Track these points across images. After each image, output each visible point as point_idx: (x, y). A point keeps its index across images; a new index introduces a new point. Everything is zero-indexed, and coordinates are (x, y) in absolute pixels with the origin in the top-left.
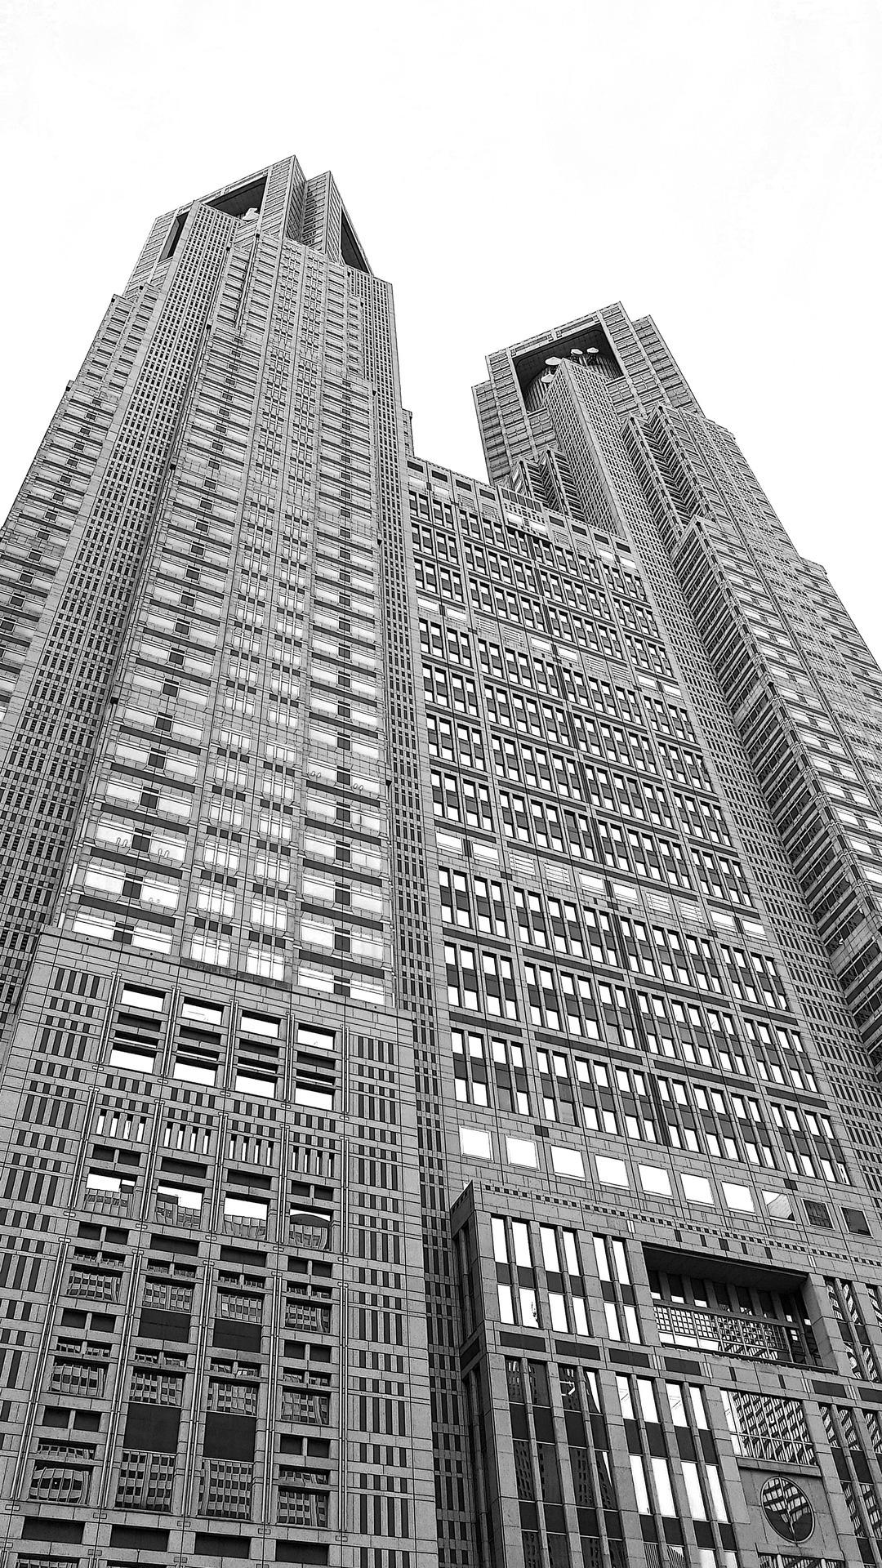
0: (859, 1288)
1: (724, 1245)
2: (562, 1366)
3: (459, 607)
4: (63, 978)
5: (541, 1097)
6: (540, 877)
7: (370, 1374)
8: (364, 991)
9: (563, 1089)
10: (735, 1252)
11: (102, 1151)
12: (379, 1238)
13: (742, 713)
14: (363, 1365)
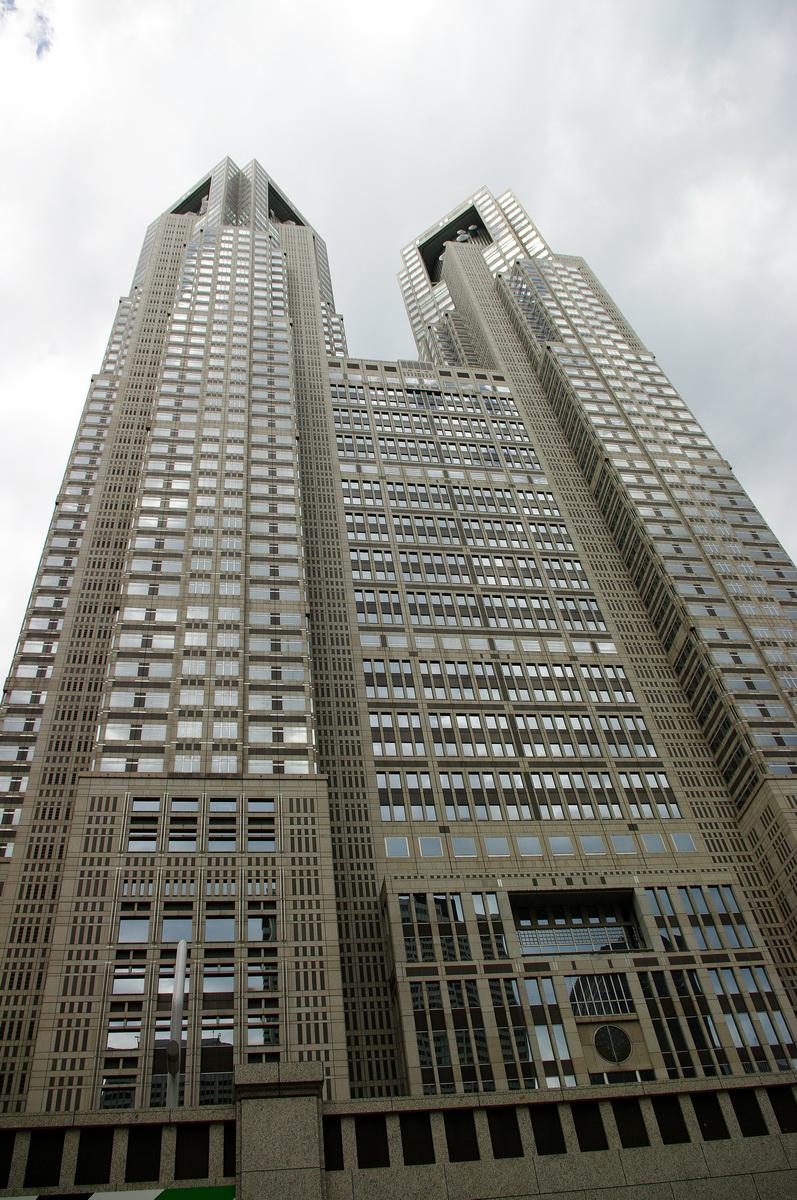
0: (673, 890)
1: (569, 881)
2: (450, 983)
3: (372, 462)
4: (96, 803)
5: (443, 805)
6: (439, 648)
7: (303, 1010)
8: (298, 767)
10: (578, 885)
11: (127, 906)
12: (307, 927)
13: (594, 484)
14: (299, 1005)
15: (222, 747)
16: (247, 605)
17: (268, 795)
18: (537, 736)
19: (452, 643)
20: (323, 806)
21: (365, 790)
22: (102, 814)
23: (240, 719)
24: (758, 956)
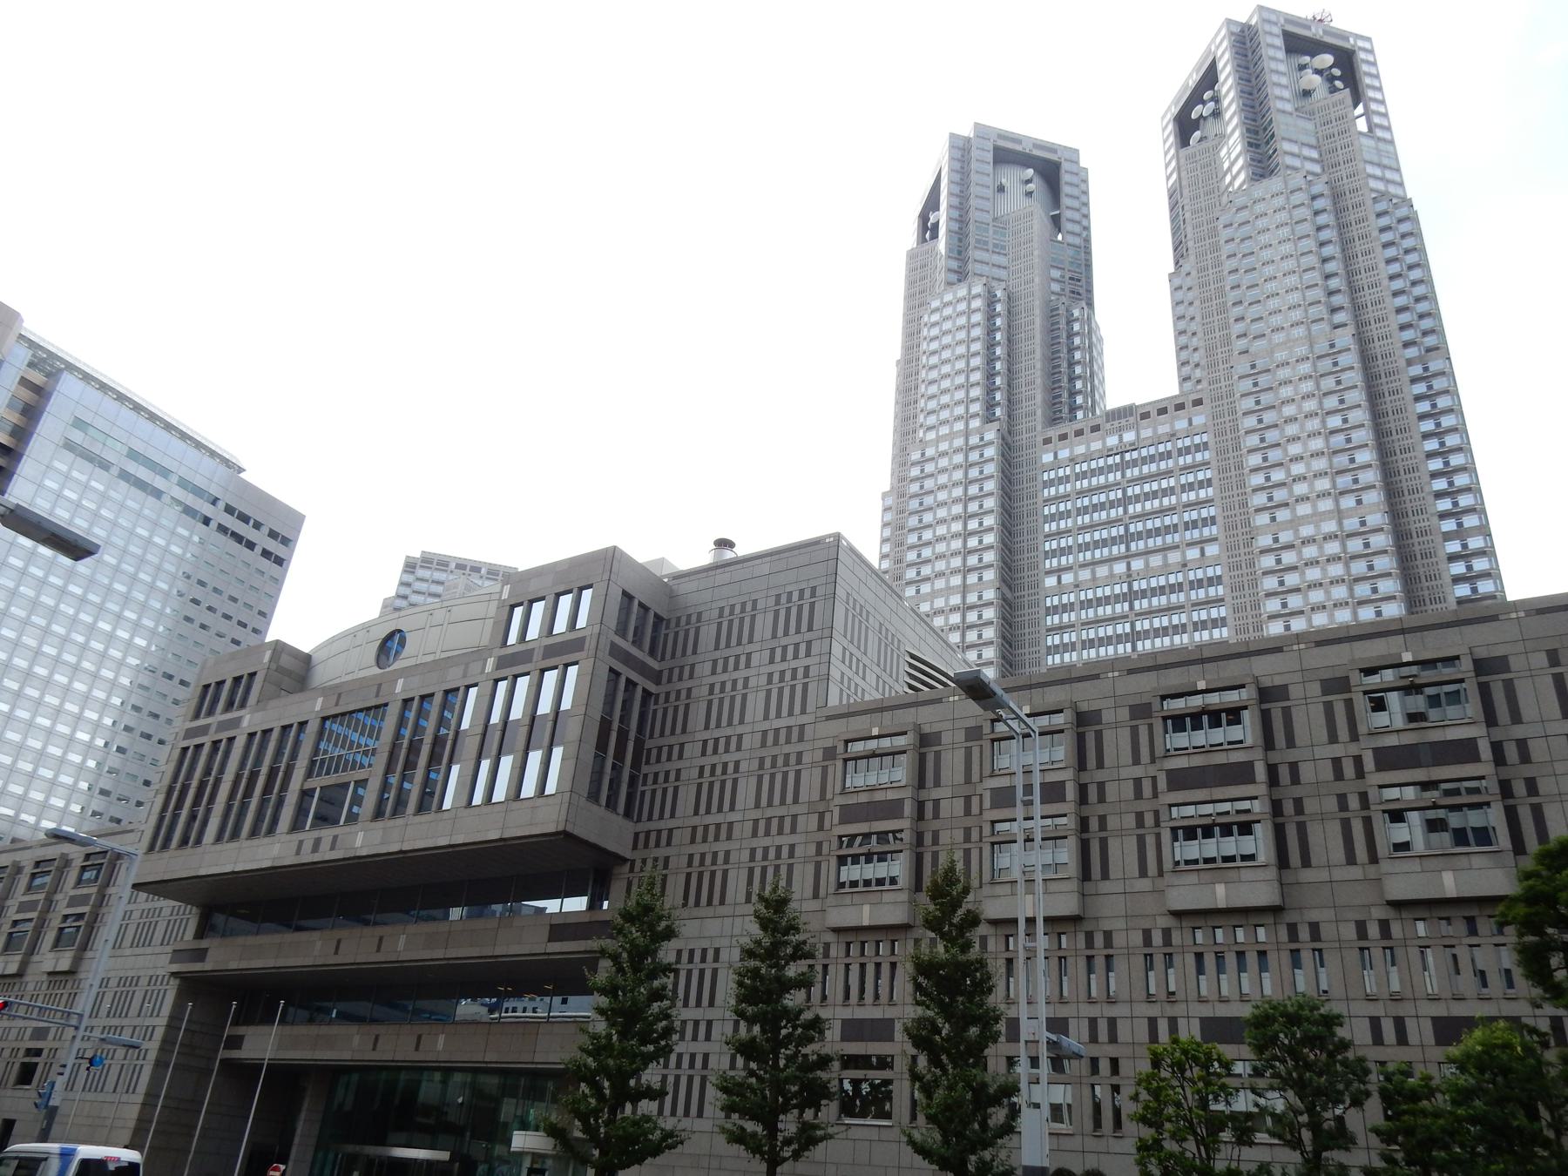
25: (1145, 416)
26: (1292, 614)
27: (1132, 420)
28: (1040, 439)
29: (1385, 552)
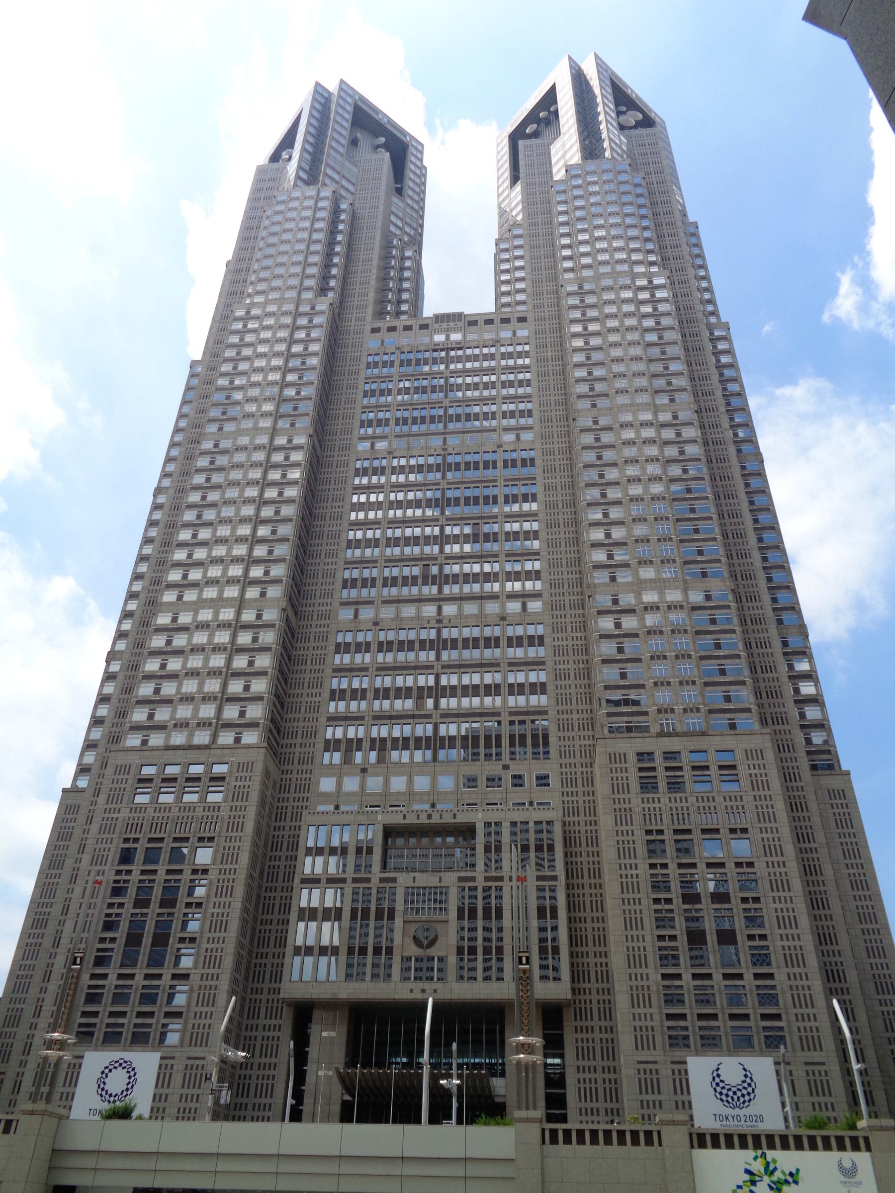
8: (251, 737)
9: (381, 745)
15: (203, 724)
16: (241, 604)
17: (225, 760)
18: (452, 691)
19: (409, 611)
20: (259, 769)
21: (316, 741)
22: (121, 777)
23: (218, 702)
24: (555, 878)
25: (473, 323)
26: (608, 484)
27: (460, 324)
28: (368, 328)
29: (695, 441)
